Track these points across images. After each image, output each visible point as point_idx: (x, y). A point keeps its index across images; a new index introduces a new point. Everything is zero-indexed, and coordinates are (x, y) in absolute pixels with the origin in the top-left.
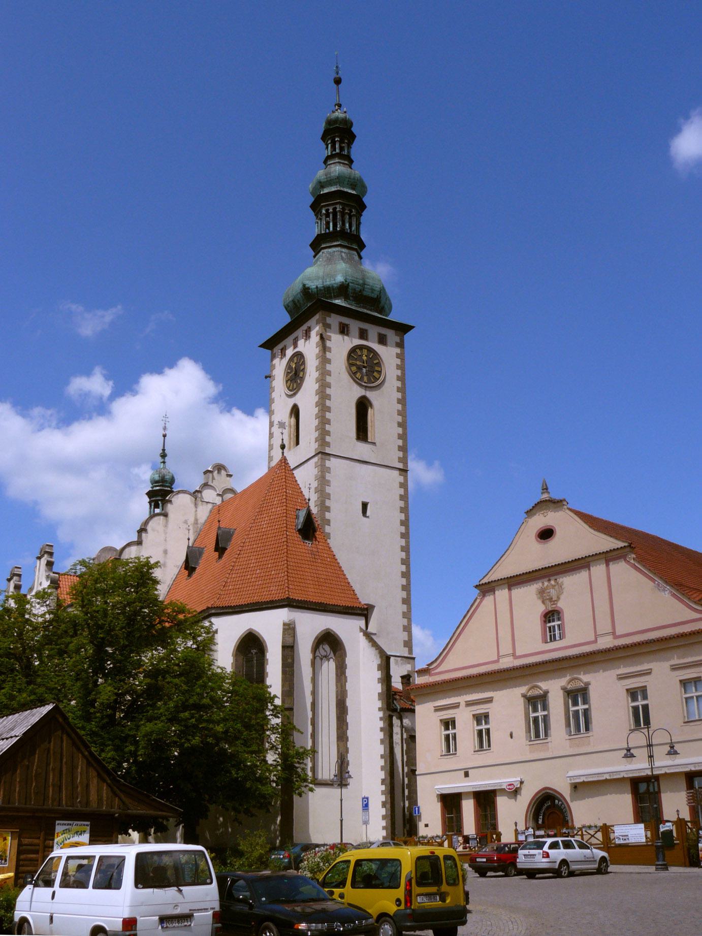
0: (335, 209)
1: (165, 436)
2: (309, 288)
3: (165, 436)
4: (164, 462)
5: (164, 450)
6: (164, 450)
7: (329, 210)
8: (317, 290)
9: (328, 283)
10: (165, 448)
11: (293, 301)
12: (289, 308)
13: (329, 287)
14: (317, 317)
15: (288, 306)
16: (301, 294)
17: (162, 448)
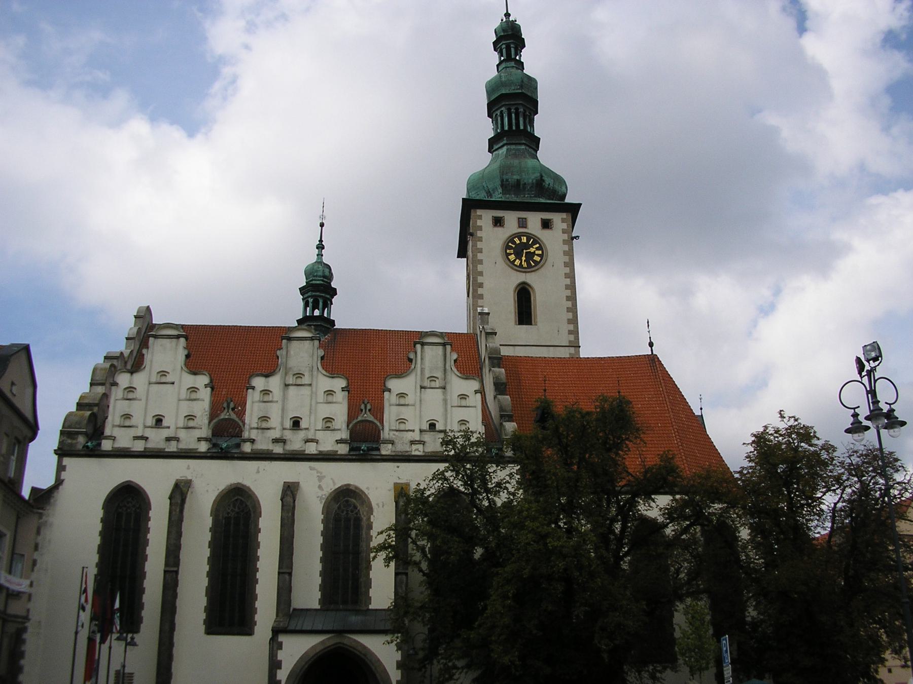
0: (517, 109)
1: (322, 225)
2: (544, 181)
3: (322, 225)
4: (320, 255)
5: (321, 241)
6: (321, 241)
7: (518, 109)
8: (548, 188)
9: (556, 187)
10: (323, 239)
11: (517, 180)
12: (508, 183)
13: (556, 191)
14: (564, 215)
15: (507, 180)
16: (534, 181)
17: (319, 239)
